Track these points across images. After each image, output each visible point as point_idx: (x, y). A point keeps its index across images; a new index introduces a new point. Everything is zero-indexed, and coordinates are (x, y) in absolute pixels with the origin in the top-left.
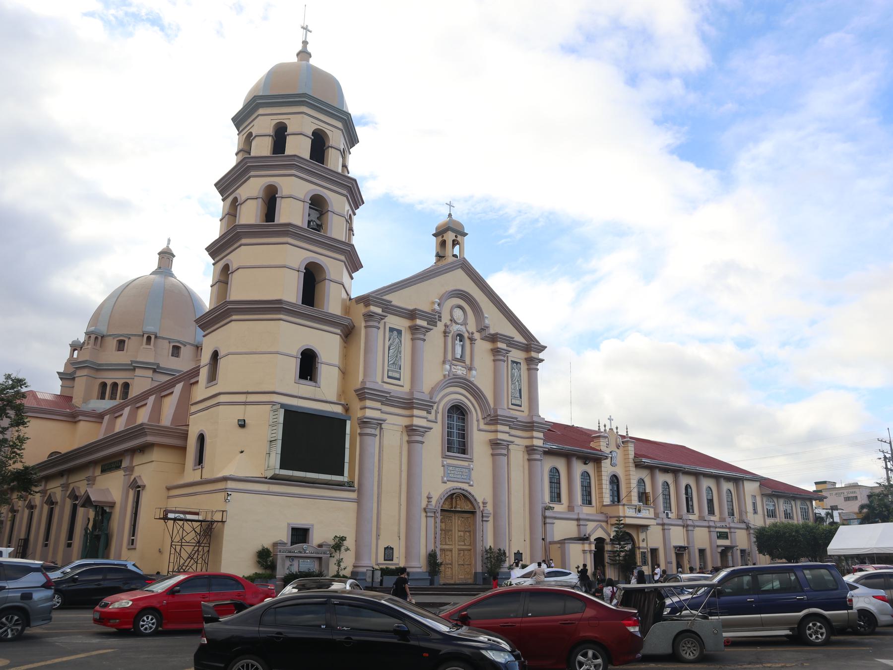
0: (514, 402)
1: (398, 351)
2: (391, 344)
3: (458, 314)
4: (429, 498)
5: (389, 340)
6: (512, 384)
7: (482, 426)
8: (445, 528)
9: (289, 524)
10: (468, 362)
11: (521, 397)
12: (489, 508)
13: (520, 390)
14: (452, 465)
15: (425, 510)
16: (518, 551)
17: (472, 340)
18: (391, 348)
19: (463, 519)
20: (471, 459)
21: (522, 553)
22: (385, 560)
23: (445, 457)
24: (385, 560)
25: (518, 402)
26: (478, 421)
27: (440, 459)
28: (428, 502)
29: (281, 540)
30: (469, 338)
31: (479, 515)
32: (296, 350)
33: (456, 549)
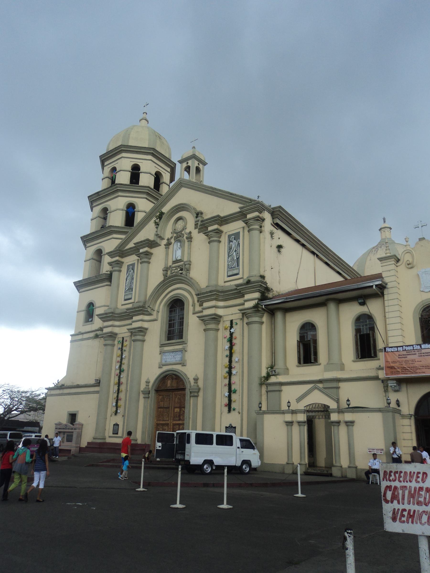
0: (230, 273)
1: (132, 278)
2: (128, 276)
3: (180, 224)
4: (148, 382)
5: (127, 274)
6: (229, 256)
7: (198, 308)
8: (164, 405)
9: (68, 412)
10: (185, 259)
11: (238, 265)
12: (201, 383)
13: (238, 259)
14: (166, 352)
15: (144, 392)
16: (231, 425)
17: (190, 238)
18: (128, 279)
19: (180, 397)
20: (183, 342)
21: (235, 428)
22: (113, 434)
23: (162, 345)
24: (113, 434)
25: (235, 272)
26: (194, 305)
27: (158, 349)
28: (146, 385)
29: (60, 422)
30: (187, 238)
31: (187, 392)
32: (84, 307)
33: (172, 424)
